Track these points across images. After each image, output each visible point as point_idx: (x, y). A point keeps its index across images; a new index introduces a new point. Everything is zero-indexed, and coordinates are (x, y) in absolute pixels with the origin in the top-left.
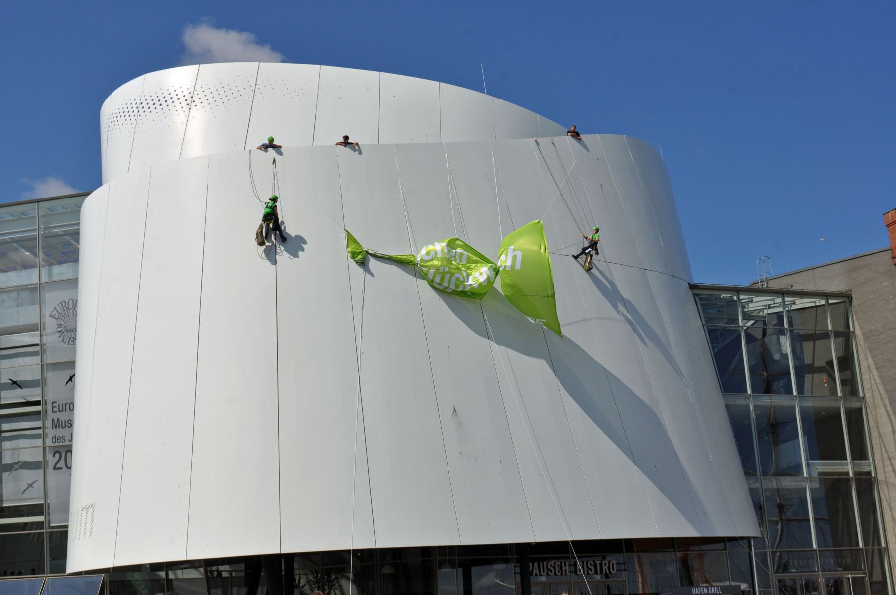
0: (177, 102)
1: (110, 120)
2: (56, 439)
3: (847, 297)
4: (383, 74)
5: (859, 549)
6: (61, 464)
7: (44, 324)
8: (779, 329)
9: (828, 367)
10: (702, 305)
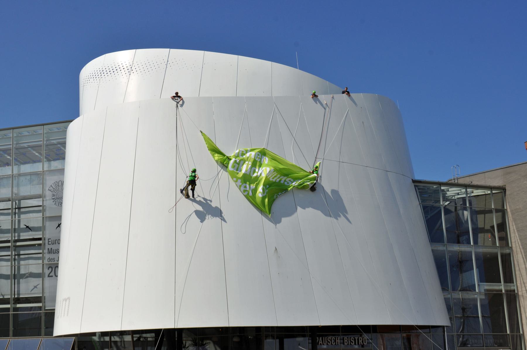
0: (123, 71)
3: (503, 189)
5: (507, 335)
8: (464, 207)
9: (491, 229)
10: (419, 192)
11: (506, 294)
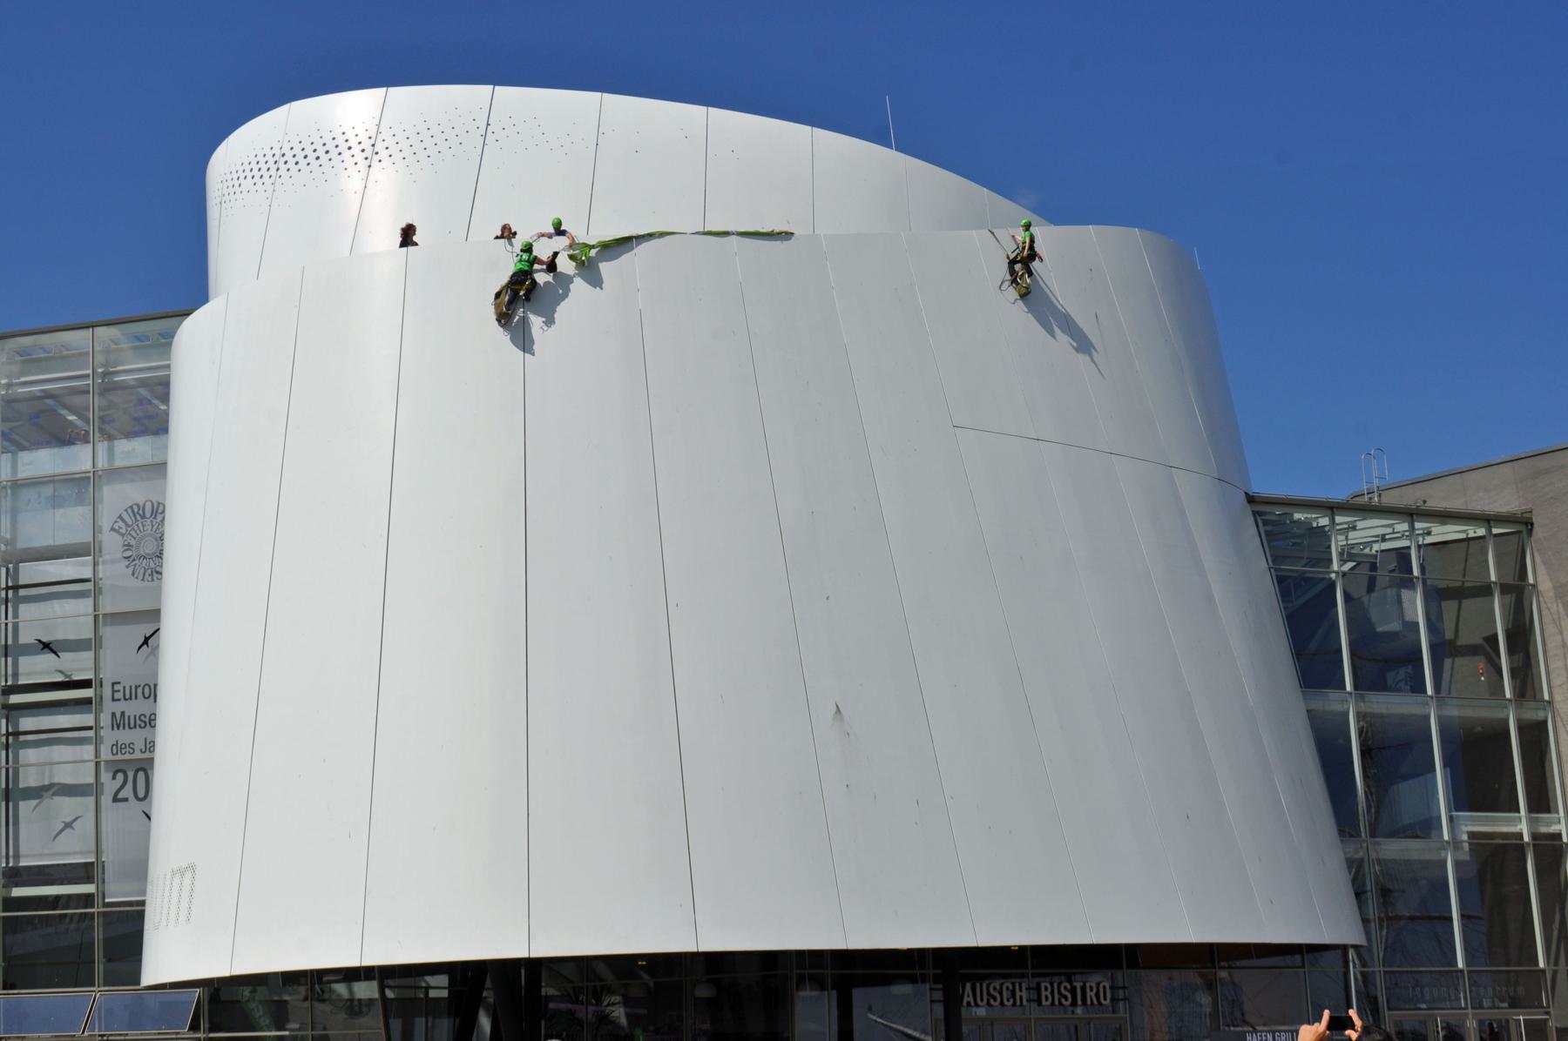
1: (225, 185)
2: (117, 747)
3: (1524, 524)
4: (711, 109)
6: (127, 792)
7: (100, 542)
8: (1402, 579)
11: (1534, 845)
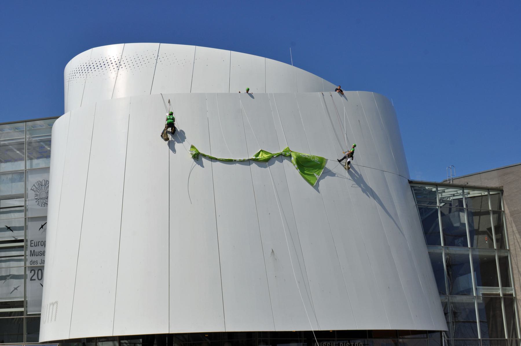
0: (111, 65)
1: (70, 75)
2: (32, 262)
3: (500, 191)
6: (35, 277)
7: (27, 194)
8: (460, 209)
9: (488, 232)
